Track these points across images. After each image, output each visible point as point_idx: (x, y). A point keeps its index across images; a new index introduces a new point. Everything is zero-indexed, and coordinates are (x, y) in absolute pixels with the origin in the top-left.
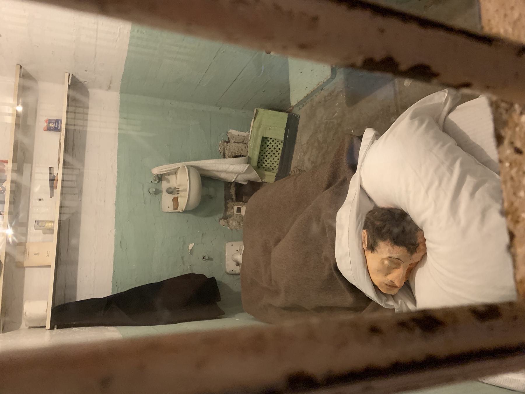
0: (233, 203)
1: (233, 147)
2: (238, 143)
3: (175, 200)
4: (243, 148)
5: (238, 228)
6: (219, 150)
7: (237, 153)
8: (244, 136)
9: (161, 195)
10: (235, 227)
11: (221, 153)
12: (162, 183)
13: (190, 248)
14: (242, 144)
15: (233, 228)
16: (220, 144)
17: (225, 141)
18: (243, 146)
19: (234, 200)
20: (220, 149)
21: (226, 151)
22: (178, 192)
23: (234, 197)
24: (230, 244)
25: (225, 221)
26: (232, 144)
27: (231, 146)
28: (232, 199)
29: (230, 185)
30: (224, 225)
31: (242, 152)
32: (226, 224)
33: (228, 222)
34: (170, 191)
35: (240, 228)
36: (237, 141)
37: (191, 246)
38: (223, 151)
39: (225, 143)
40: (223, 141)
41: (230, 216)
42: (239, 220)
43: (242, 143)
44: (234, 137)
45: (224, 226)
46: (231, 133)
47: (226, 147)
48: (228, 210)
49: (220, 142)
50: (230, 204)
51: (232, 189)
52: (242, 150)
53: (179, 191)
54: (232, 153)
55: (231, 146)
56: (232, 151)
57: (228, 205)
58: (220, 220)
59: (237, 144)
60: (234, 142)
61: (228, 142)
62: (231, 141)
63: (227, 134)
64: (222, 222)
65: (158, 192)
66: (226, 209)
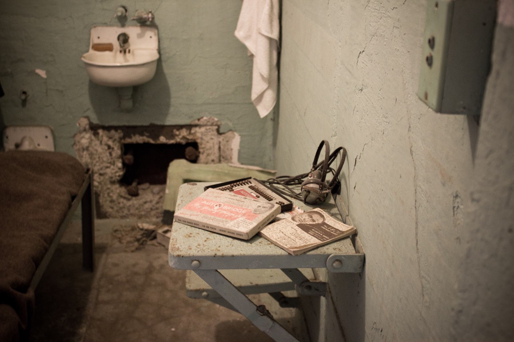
0: (118, 139)
1: (211, 141)
2: (220, 148)
3: (108, 48)
4: (212, 157)
5: (78, 147)
6: (202, 118)
7: (203, 146)
8: (231, 158)
9: (117, 26)
10: (79, 142)
11: (199, 120)
12: (137, 26)
13: (38, 71)
14: (217, 155)
15: (77, 138)
16: (213, 119)
17: (219, 127)
18: (215, 156)
19: (123, 141)
20: (205, 118)
21: (203, 129)
22: (123, 52)
23: (128, 141)
24: (48, 133)
25: (87, 127)
26: (216, 139)
27: (213, 137)
28: (124, 137)
29: (147, 134)
30: (79, 124)
31: (205, 154)
32: (82, 129)
33: (85, 130)
34: (124, 39)
35: (79, 150)
36: (222, 147)
37: (42, 73)
38: (202, 123)
39: (216, 127)
40: (219, 123)
41: (96, 134)
42: (90, 149)
43: (220, 156)
44: (227, 141)
45: (78, 125)
46: (233, 138)
47: (210, 129)
48: (106, 132)
49: (216, 119)
50: (117, 135)
51: (141, 138)
52: (208, 155)
53: (125, 52)
54: (202, 139)
55: (213, 137)
56: (204, 137)
57: (113, 132)
58: (87, 117)
59: (217, 147)
60: (220, 142)
61: (219, 133)
62: (221, 138)
63: (231, 130)
64: (84, 122)
65: (122, 20)
66: (108, 129)
